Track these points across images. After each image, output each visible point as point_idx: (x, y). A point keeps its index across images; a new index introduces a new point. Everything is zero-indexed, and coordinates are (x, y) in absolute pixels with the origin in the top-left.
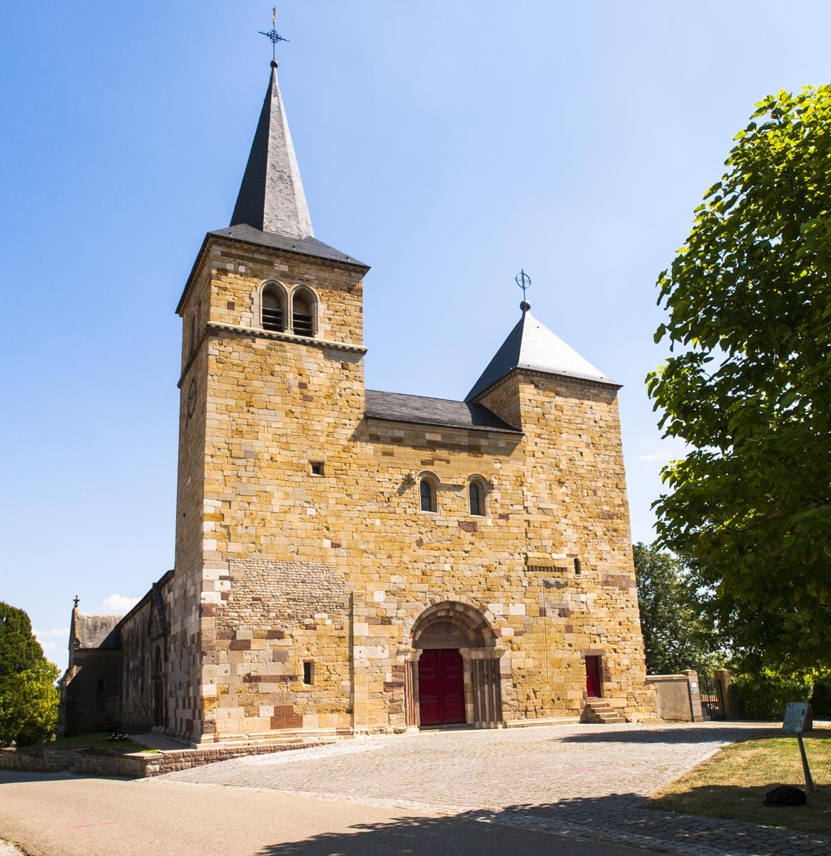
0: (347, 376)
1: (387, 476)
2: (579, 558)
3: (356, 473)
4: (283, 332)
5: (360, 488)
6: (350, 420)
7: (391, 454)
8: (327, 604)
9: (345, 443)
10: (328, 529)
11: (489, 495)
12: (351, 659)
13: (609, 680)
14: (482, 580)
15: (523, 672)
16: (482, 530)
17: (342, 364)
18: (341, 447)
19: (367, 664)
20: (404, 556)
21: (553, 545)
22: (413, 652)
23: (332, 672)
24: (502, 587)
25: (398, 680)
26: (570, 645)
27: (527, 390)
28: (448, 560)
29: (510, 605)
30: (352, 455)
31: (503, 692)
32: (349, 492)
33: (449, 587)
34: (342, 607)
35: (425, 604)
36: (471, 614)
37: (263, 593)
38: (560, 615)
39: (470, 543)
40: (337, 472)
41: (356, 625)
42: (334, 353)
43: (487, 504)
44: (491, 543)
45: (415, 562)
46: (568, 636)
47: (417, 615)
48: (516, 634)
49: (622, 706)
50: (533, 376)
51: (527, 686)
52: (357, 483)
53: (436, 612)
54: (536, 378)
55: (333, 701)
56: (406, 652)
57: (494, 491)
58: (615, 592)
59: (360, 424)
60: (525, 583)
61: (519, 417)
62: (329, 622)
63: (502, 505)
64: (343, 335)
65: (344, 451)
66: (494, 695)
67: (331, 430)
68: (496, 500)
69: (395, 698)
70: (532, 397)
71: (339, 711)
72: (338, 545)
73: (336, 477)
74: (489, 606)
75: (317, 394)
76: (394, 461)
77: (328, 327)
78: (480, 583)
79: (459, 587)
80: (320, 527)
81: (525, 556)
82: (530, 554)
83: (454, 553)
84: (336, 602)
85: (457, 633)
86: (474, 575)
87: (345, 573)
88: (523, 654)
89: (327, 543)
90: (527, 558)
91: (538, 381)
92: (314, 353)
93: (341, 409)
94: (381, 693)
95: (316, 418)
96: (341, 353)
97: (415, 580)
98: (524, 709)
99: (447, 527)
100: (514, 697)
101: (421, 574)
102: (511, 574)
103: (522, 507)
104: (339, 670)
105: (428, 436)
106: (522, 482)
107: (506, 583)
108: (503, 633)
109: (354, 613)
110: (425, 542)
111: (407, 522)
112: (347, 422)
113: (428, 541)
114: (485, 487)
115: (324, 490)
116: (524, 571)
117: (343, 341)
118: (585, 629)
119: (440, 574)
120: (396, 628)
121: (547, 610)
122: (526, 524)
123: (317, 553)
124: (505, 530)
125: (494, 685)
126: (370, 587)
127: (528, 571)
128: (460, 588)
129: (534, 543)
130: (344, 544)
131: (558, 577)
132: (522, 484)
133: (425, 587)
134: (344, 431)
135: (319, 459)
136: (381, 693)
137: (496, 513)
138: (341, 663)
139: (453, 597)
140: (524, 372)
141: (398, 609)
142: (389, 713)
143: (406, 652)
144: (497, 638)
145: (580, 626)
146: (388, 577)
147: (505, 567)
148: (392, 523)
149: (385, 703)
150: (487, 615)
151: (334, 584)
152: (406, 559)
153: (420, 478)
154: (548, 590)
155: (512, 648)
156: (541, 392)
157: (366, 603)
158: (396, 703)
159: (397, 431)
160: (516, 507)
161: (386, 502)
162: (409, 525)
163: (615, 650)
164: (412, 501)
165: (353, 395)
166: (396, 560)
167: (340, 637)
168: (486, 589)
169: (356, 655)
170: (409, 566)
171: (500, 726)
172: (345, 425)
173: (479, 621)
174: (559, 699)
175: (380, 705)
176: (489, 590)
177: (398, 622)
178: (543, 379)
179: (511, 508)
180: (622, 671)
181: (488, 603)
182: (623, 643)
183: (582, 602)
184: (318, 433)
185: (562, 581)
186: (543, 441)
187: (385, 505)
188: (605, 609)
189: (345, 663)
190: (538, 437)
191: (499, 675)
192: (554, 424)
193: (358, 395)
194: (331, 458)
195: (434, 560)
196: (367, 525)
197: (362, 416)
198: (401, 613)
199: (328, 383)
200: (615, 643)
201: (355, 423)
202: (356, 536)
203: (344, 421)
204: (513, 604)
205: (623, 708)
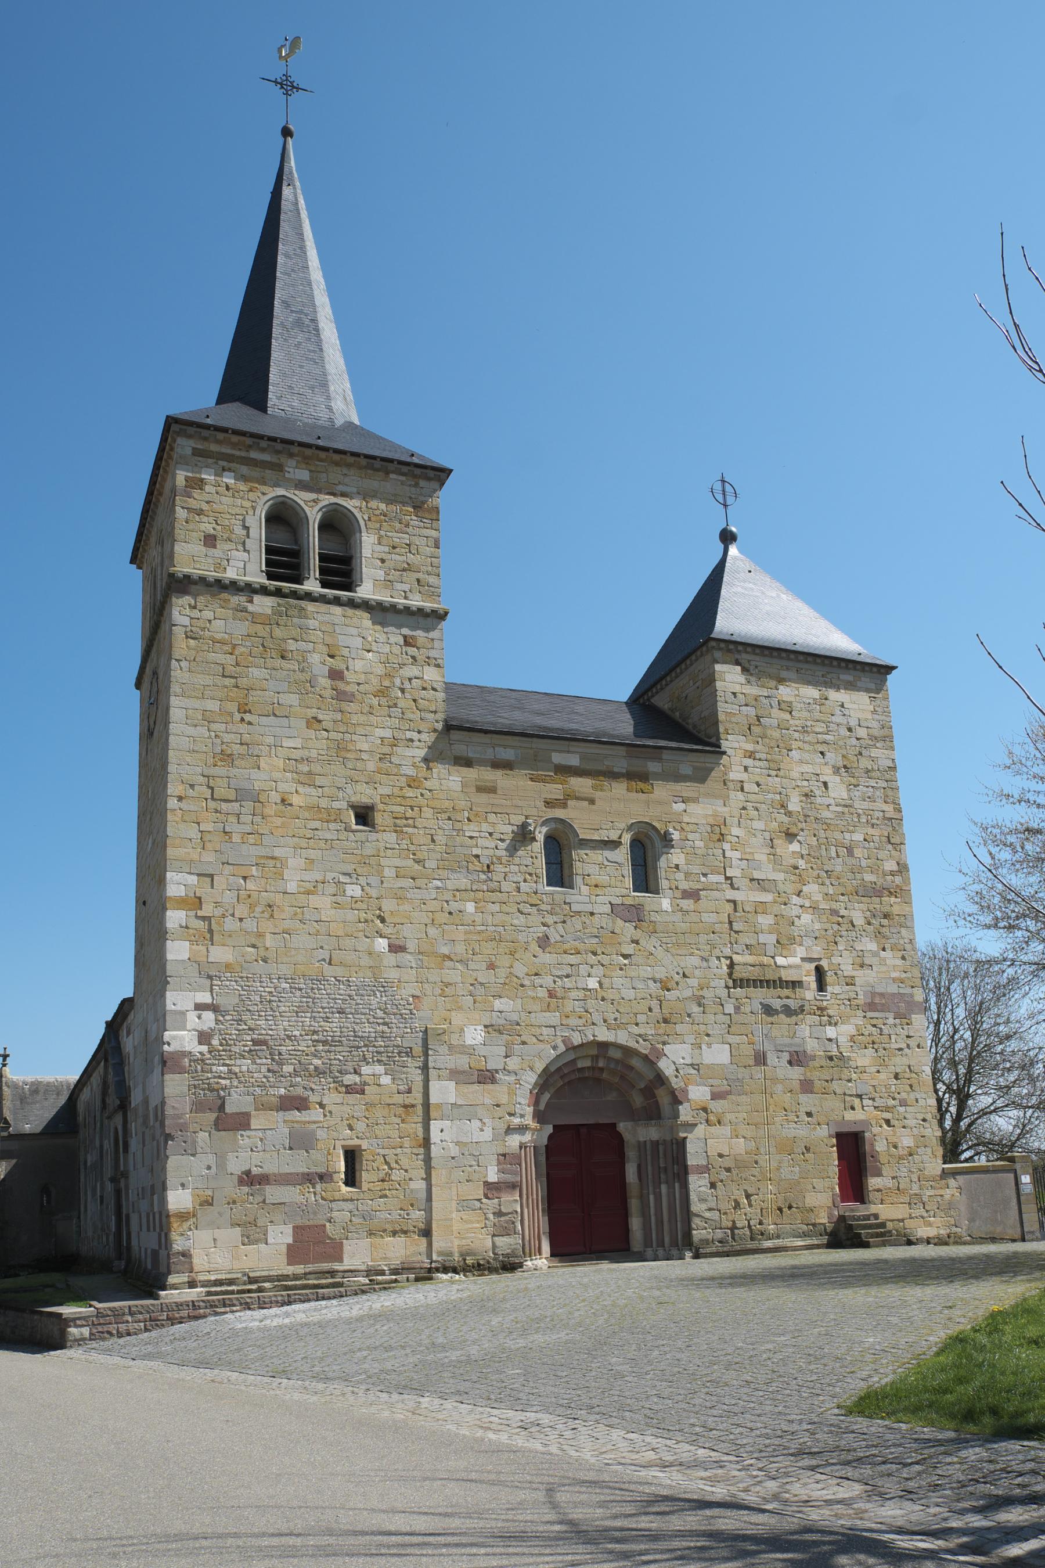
0: (413, 657)
1: (485, 827)
2: (824, 963)
3: (432, 823)
4: (302, 584)
5: (438, 848)
6: (419, 732)
7: (492, 790)
8: (382, 1049)
9: (411, 772)
10: (383, 920)
11: (664, 856)
12: (426, 1143)
13: (879, 1174)
14: (655, 1004)
15: (728, 1163)
16: (652, 919)
17: (405, 637)
18: (404, 779)
19: (454, 1151)
20: (516, 964)
21: (778, 942)
22: (535, 1130)
23: (394, 1165)
24: (689, 1016)
25: (509, 1178)
26: (809, 1114)
27: (728, 677)
28: (593, 971)
29: (704, 1047)
30: (424, 792)
31: (693, 1197)
32: (420, 856)
33: (597, 1018)
34: (409, 1052)
35: (555, 1048)
36: (635, 1062)
37: (270, 1032)
38: (790, 1063)
39: (633, 942)
40: (398, 821)
41: (434, 1086)
42: (390, 616)
43: (662, 873)
44: (668, 940)
45: (536, 974)
46: (803, 1098)
47: (540, 1067)
48: (715, 1096)
49: (900, 1217)
50: (739, 652)
51: (734, 1187)
52: (433, 841)
53: (574, 1061)
54: (744, 656)
55: (395, 1215)
56: (522, 1129)
57: (672, 851)
59: (436, 738)
60: (729, 1008)
61: (716, 723)
62: (386, 1080)
63: (687, 875)
64: (406, 587)
65: (409, 786)
66: (678, 1202)
67: (387, 750)
68: (677, 867)
69: (504, 1210)
70: (737, 689)
71: (405, 1232)
72: (400, 947)
73: (396, 831)
74: (667, 1049)
75: (362, 688)
76: (496, 801)
77: (380, 574)
78: (650, 1010)
79: (613, 1016)
80: (370, 917)
81: (728, 962)
82: (737, 958)
83: (605, 960)
84: (398, 1046)
85: (612, 1096)
86: (639, 996)
87: (413, 996)
88: (727, 1130)
89: (382, 944)
90: (731, 966)
91: (749, 661)
92: (355, 620)
93: (403, 713)
94: (479, 1200)
95: (360, 730)
96: (402, 618)
97: (536, 1007)
98: (730, 1224)
99: (592, 914)
100: (713, 1205)
101: (547, 995)
102: (705, 993)
103: (722, 879)
104: (405, 1162)
105: (557, 758)
106: (722, 835)
107: (696, 1009)
108: (691, 1096)
109: (431, 1065)
110: (552, 941)
111: (521, 906)
112: (415, 736)
113: (558, 938)
114: (658, 843)
115: (375, 853)
116: (727, 987)
117: (406, 598)
118: (836, 1086)
119: (581, 994)
120: (505, 1089)
121: (769, 1055)
122: (729, 907)
123: (366, 961)
124: (694, 917)
125: (677, 1185)
126: (457, 1018)
127: (734, 988)
128: (615, 1019)
129: (746, 939)
130: (411, 946)
131: (788, 997)
132: (722, 837)
133: (554, 1018)
134: (409, 752)
135: (365, 800)
136: (479, 1200)
137: (677, 888)
138: (408, 1151)
139: (603, 1035)
140: (722, 645)
141: (506, 1057)
142: (494, 1235)
143: (522, 1129)
144: (681, 1103)
145: (827, 1081)
146: (490, 1001)
147: (693, 982)
148: (496, 908)
149: (486, 1219)
150: (665, 1066)
151: (394, 1014)
152: (520, 970)
153: (544, 829)
154: (770, 1019)
155: (707, 1121)
156: (753, 679)
157: (451, 1047)
158: (507, 1218)
159: (501, 749)
160: (714, 878)
161: (483, 872)
162: (525, 911)
163: (888, 1122)
164: (530, 869)
165: (424, 689)
166: (502, 973)
167: (405, 1106)
168: (661, 1020)
169: (435, 1136)
170: (527, 982)
171: (688, 1254)
172: (412, 740)
173: (651, 1076)
174: (790, 1207)
176: (666, 1021)
177: (506, 1078)
178: (757, 658)
179: (703, 879)
180: (901, 1158)
181: (664, 1043)
182: (902, 1109)
183: (830, 1040)
184: (364, 756)
185: (791, 1003)
186: (758, 763)
187: (483, 877)
189: (415, 1151)
190: (750, 757)
191: (686, 1167)
192: (776, 734)
193: (434, 689)
194: (386, 799)
195: (568, 970)
196: (450, 913)
197: (440, 726)
198: (513, 1063)
199: (380, 670)
200: (888, 1109)
201: (428, 738)
202: (432, 931)
203: (409, 735)
204: (709, 1045)
205: (902, 1220)
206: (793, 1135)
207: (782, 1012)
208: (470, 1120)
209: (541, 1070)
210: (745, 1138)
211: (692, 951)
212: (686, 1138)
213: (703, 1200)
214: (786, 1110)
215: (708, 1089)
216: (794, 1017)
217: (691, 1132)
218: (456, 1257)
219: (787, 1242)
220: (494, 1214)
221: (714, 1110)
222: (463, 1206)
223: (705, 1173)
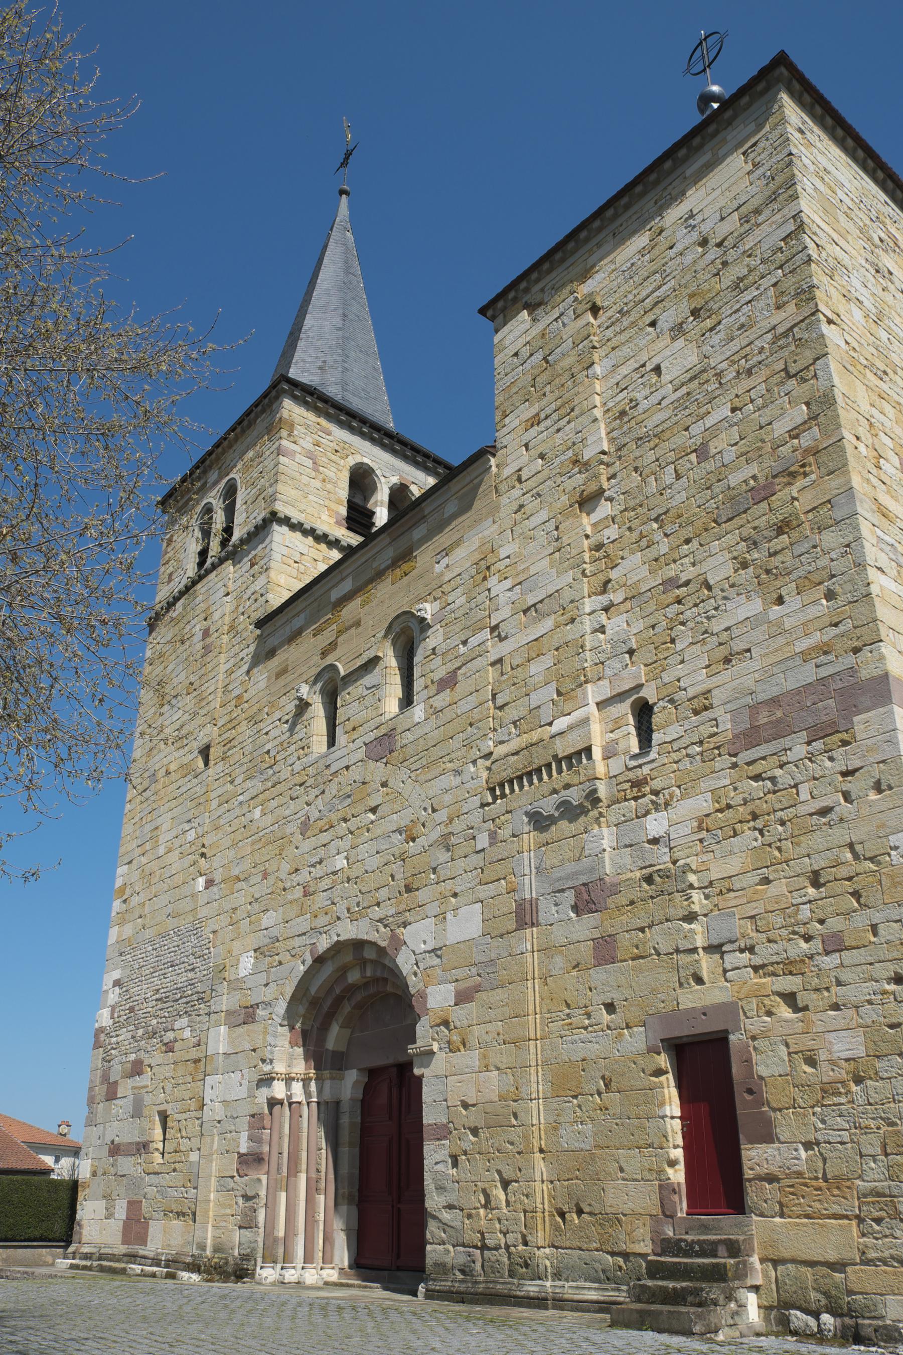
2: (649, 694)
13: (767, 1136)
15: (473, 1117)
21: (559, 693)
26: (610, 1008)
29: (449, 916)
38: (576, 908)
46: (598, 975)
49: (832, 1256)
57: (431, 631)
58: (791, 756)
69: (249, 1194)
88: (470, 1058)
94: (232, 1177)
118: (657, 937)
139: (348, 931)
145: (642, 930)
154: (545, 836)
163: (790, 998)
174: (580, 1212)
175: (230, 1206)
176: (408, 889)
180: (830, 1089)
181: (405, 925)
182: (830, 961)
183: (655, 841)
185: (575, 796)
188: (749, 838)
200: (790, 967)
205: (839, 1266)
206: (581, 1056)
207: (562, 817)
209: (290, 995)
210: (498, 1069)
211: (443, 766)
212: (423, 1075)
213: (441, 1189)
214: (568, 1006)
215: (451, 987)
216: (582, 819)
217: (427, 1066)
218: (209, 1252)
219: (568, 1289)
220: (243, 1196)
221: (458, 1024)
222: (221, 1185)
223: (445, 1138)
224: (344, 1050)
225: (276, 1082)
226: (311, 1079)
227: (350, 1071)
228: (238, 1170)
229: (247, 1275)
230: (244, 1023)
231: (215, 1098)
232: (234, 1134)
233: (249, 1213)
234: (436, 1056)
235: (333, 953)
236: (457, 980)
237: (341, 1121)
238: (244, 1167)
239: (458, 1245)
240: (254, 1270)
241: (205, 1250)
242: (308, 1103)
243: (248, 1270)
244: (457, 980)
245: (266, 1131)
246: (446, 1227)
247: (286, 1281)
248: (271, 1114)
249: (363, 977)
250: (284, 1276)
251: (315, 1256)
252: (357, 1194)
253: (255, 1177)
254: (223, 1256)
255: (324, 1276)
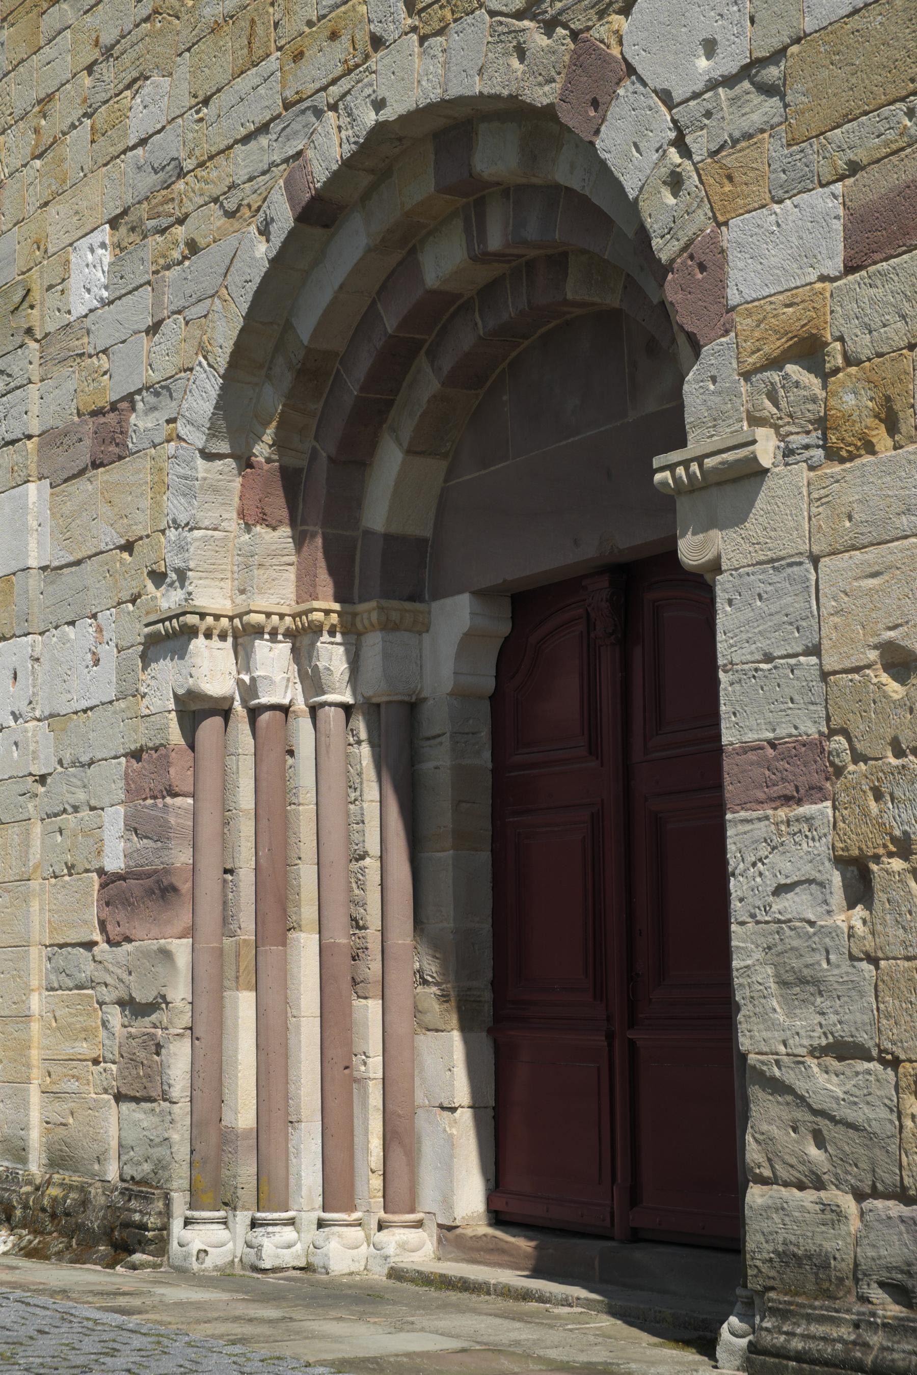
94: (89, 945)
175: (87, 1034)
208: (72, 623)
209: (229, 346)
212: (715, 567)
218: (35, 1167)
220: (121, 1003)
221: (862, 344)
223: (815, 793)
224: (428, 533)
225: (199, 643)
226: (316, 630)
227: (449, 601)
228: (102, 925)
229: (141, 1244)
230: (95, 465)
231: (23, 707)
232: (85, 813)
233: (142, 1055)
234: (769, 482)
235: (366, 180)
236: (854, 168)
237: (427, 766)
238: (121, 915)
239: (875, 1194)
240: (165, 1227)
241: (24, 1161)
242: (314, 710)
243: (143, 1227)
244: (854, 168)
245: (179, 801)
246: (824, 1124)
247: (267, 1265)
248: (192, 747)
249: (474, 259)
250: (260, 1248)
251: (360, 1188)
252: (488, 996)
253: (154, 945)
254: (76, 1179)
255: (391, 1250)
